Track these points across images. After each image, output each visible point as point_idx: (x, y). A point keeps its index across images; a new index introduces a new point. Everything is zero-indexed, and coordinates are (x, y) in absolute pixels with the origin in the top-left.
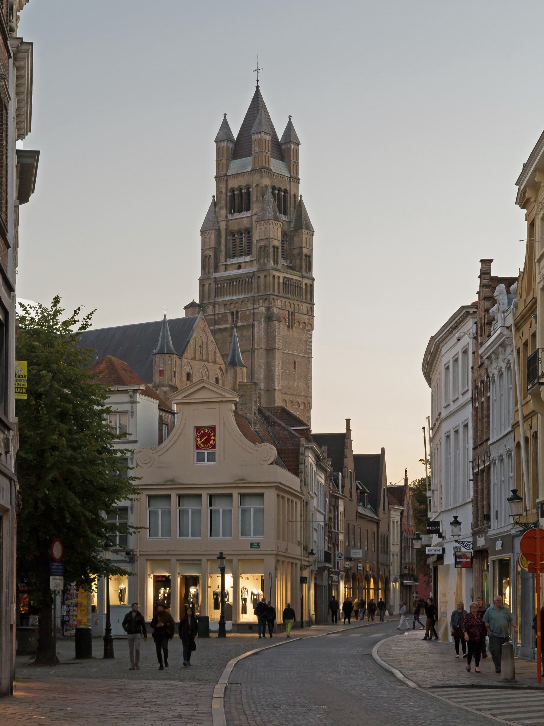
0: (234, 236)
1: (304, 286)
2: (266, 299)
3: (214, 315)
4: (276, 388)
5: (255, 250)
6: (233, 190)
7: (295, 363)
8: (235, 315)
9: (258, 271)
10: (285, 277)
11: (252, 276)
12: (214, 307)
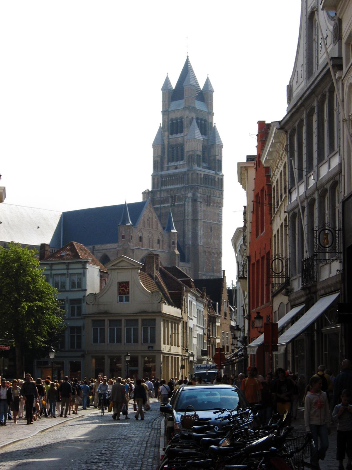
0: (173, 148)
1: (217, 180)
2: (192, 188)
3: (161, 198)
4: (199, 244)
5: (185, 157)
6: (172, 120)
7: (211, 227)
8: (173, 198)
9: (188, 170)
10: (204, 174)
11: (184, 174)
12: (160, 193)
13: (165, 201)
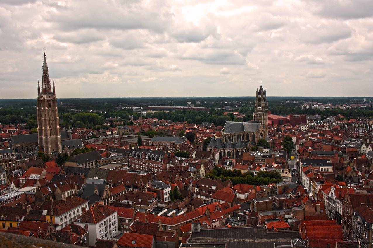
8: (259, 115)
11: (261, 110)
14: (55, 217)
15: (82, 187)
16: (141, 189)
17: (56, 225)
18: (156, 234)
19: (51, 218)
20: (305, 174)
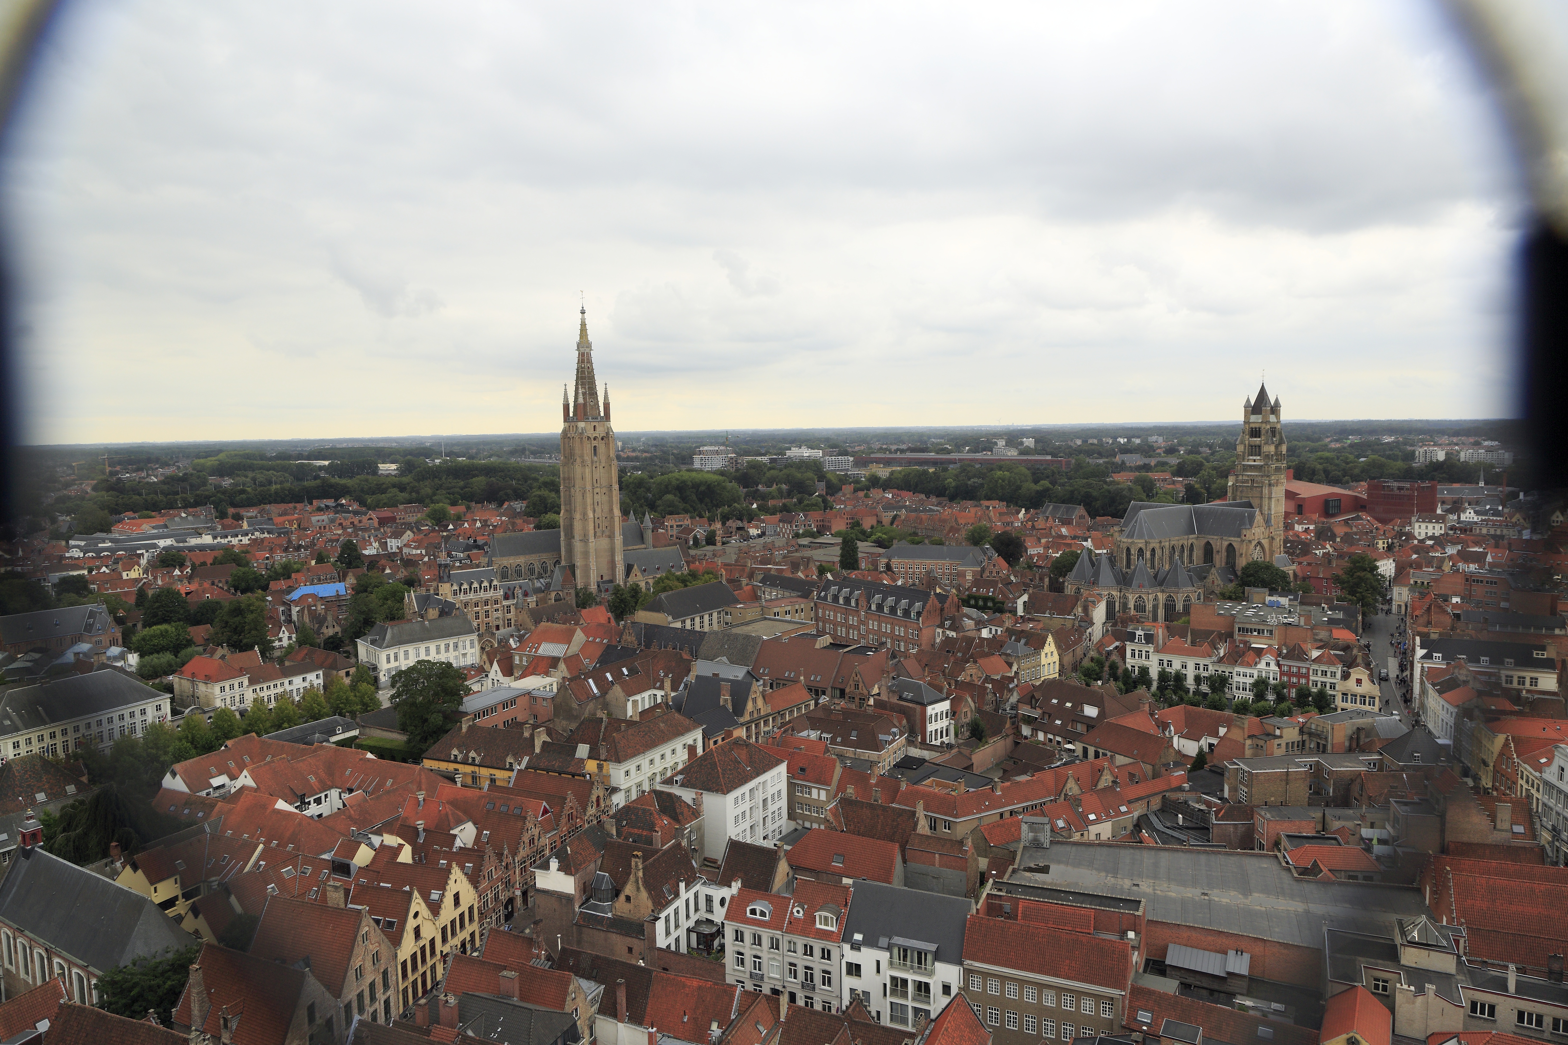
8: (1253, 481)
11: (1262, 466)
13: (1247, 481)
14: (611, 766)
15: (683, 685)
16: (857, 700)
17: (615, 790)
18: (907, 841)
19: (600, 767)
20: (1440, 692)
